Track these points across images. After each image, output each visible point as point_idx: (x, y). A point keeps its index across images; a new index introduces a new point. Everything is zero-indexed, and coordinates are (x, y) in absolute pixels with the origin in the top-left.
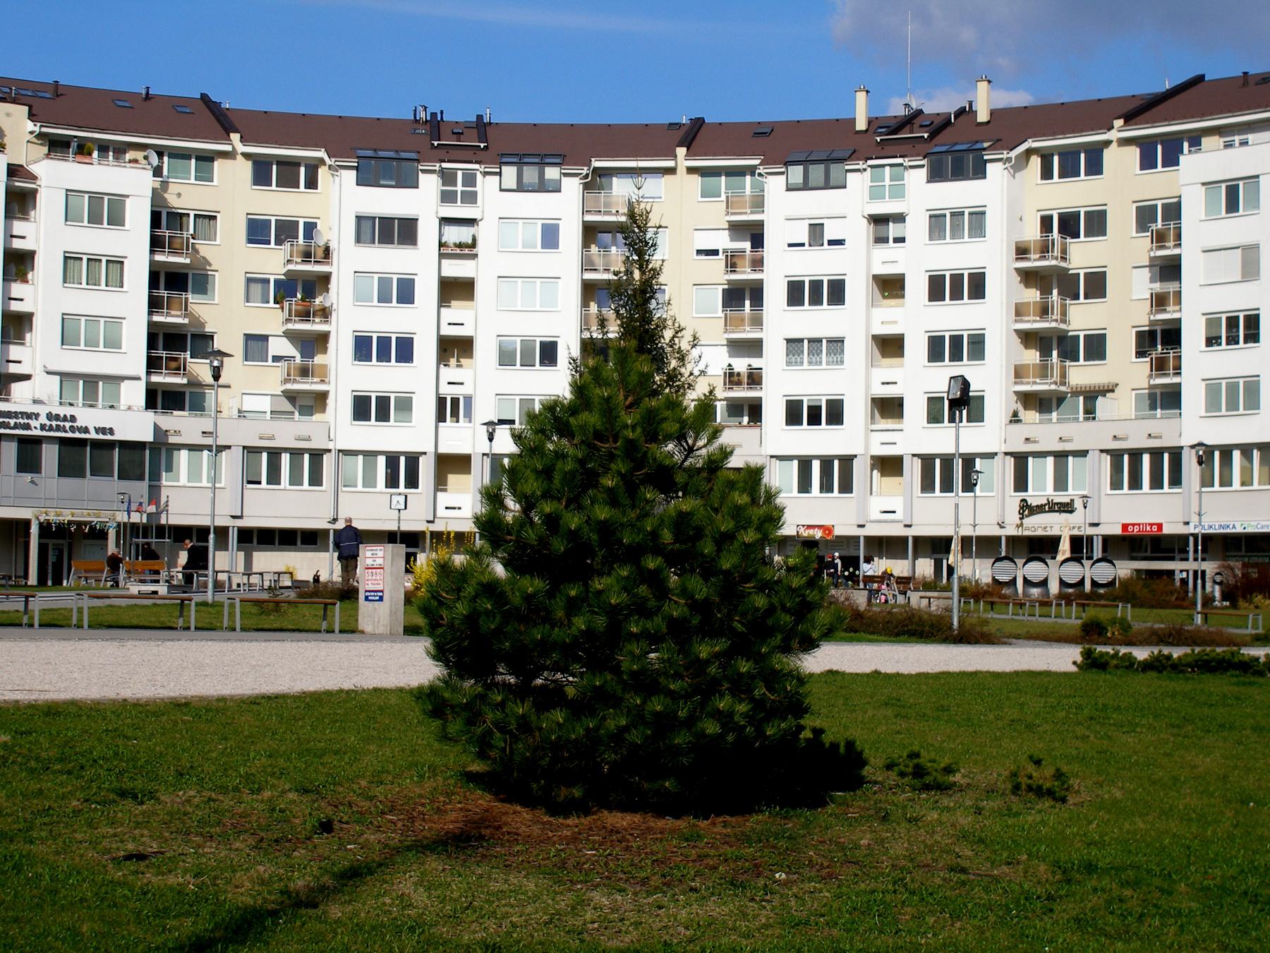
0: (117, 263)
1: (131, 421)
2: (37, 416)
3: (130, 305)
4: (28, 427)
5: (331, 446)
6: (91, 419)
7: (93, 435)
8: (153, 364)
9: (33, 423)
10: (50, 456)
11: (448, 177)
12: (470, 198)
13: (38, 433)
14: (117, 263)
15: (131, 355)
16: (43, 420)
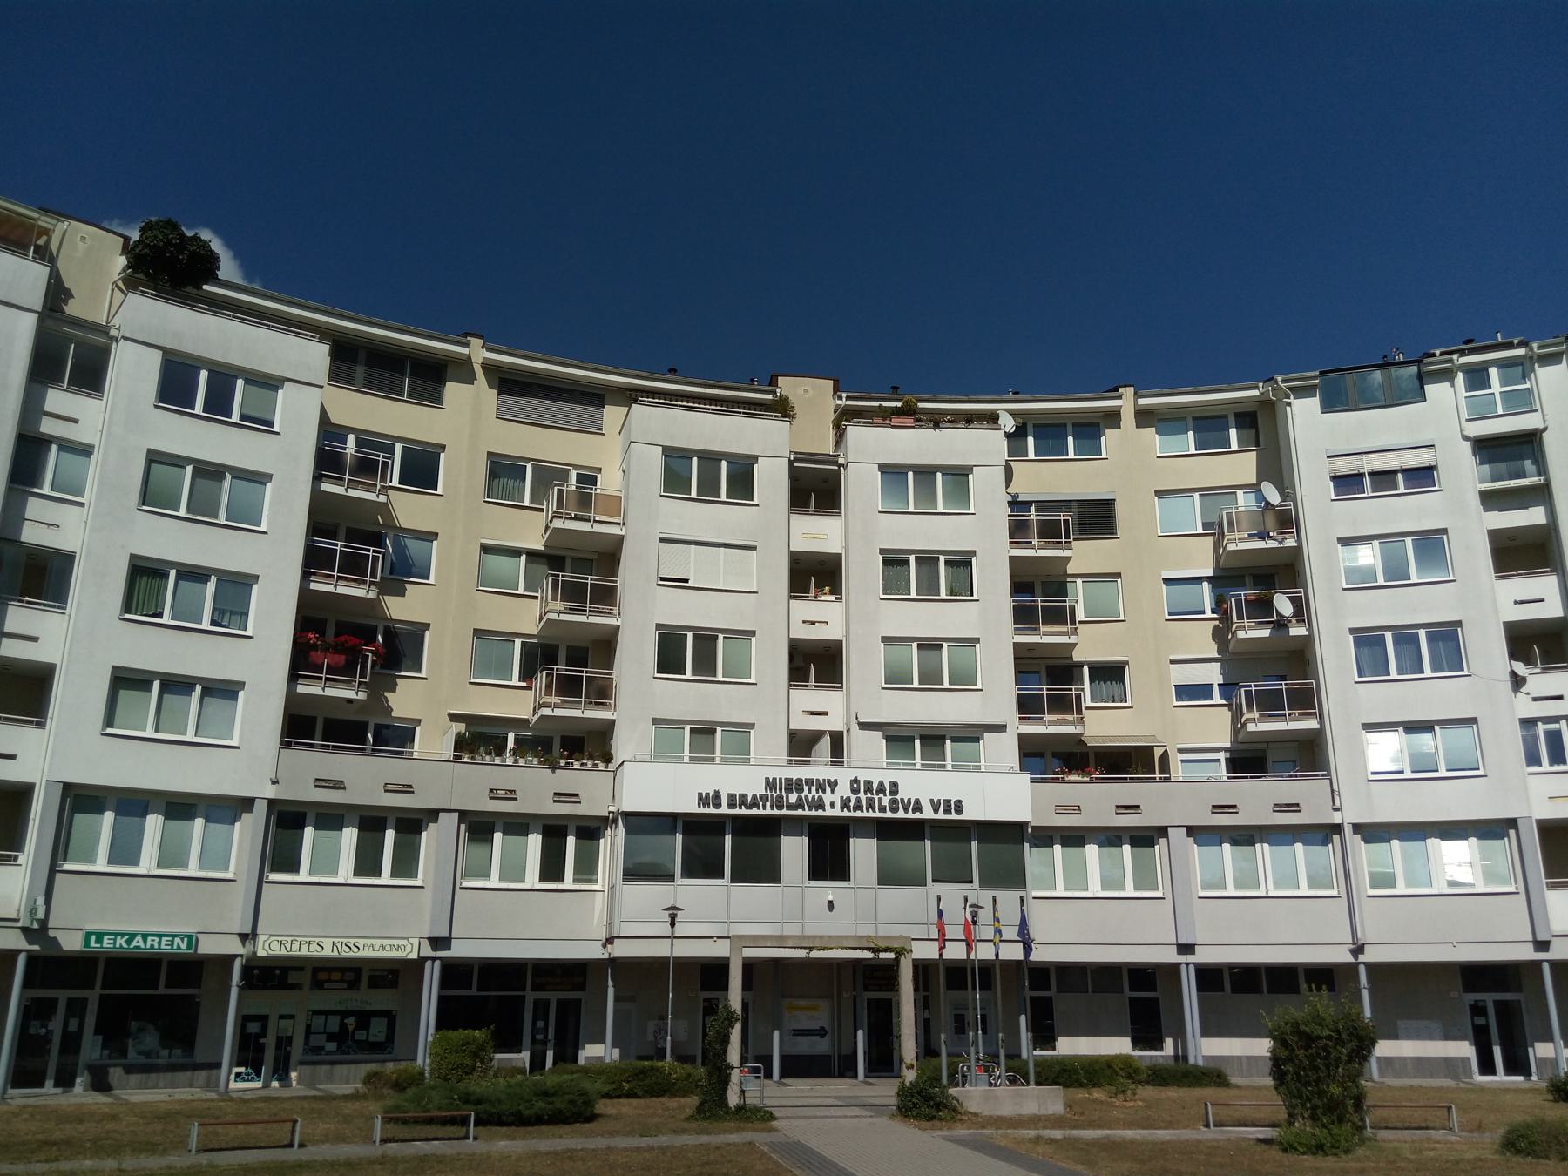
0: (961, 563)
1: (997, 789)
2: (833, 785)
3: (986, 619)
4: (821, 806)
5: (1336, 818)
6: (924, 787)
7: (928, 813)
8: (1028, 706)
9: (828, 798)
10: (863, 852)
11: (1477, 378)
12: (1521, 402)
13: (837, 812)
14: (961, 563)
15: (994, 694)
16: (844, 790)
